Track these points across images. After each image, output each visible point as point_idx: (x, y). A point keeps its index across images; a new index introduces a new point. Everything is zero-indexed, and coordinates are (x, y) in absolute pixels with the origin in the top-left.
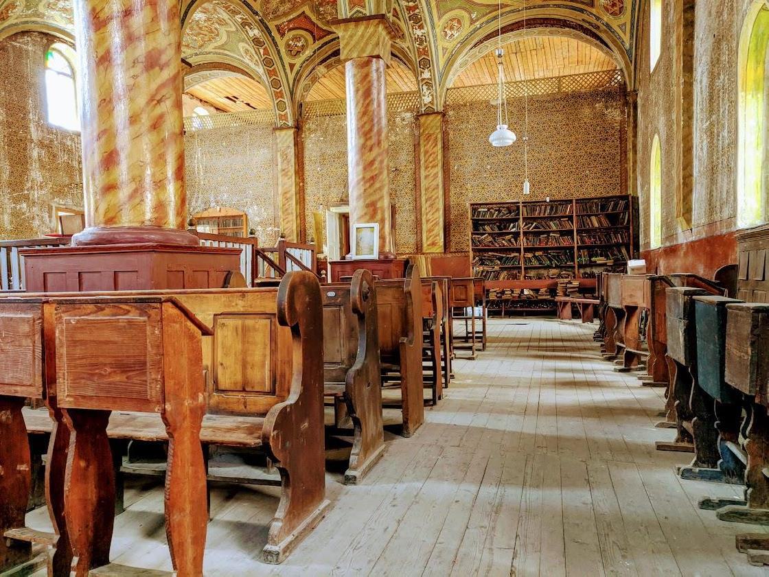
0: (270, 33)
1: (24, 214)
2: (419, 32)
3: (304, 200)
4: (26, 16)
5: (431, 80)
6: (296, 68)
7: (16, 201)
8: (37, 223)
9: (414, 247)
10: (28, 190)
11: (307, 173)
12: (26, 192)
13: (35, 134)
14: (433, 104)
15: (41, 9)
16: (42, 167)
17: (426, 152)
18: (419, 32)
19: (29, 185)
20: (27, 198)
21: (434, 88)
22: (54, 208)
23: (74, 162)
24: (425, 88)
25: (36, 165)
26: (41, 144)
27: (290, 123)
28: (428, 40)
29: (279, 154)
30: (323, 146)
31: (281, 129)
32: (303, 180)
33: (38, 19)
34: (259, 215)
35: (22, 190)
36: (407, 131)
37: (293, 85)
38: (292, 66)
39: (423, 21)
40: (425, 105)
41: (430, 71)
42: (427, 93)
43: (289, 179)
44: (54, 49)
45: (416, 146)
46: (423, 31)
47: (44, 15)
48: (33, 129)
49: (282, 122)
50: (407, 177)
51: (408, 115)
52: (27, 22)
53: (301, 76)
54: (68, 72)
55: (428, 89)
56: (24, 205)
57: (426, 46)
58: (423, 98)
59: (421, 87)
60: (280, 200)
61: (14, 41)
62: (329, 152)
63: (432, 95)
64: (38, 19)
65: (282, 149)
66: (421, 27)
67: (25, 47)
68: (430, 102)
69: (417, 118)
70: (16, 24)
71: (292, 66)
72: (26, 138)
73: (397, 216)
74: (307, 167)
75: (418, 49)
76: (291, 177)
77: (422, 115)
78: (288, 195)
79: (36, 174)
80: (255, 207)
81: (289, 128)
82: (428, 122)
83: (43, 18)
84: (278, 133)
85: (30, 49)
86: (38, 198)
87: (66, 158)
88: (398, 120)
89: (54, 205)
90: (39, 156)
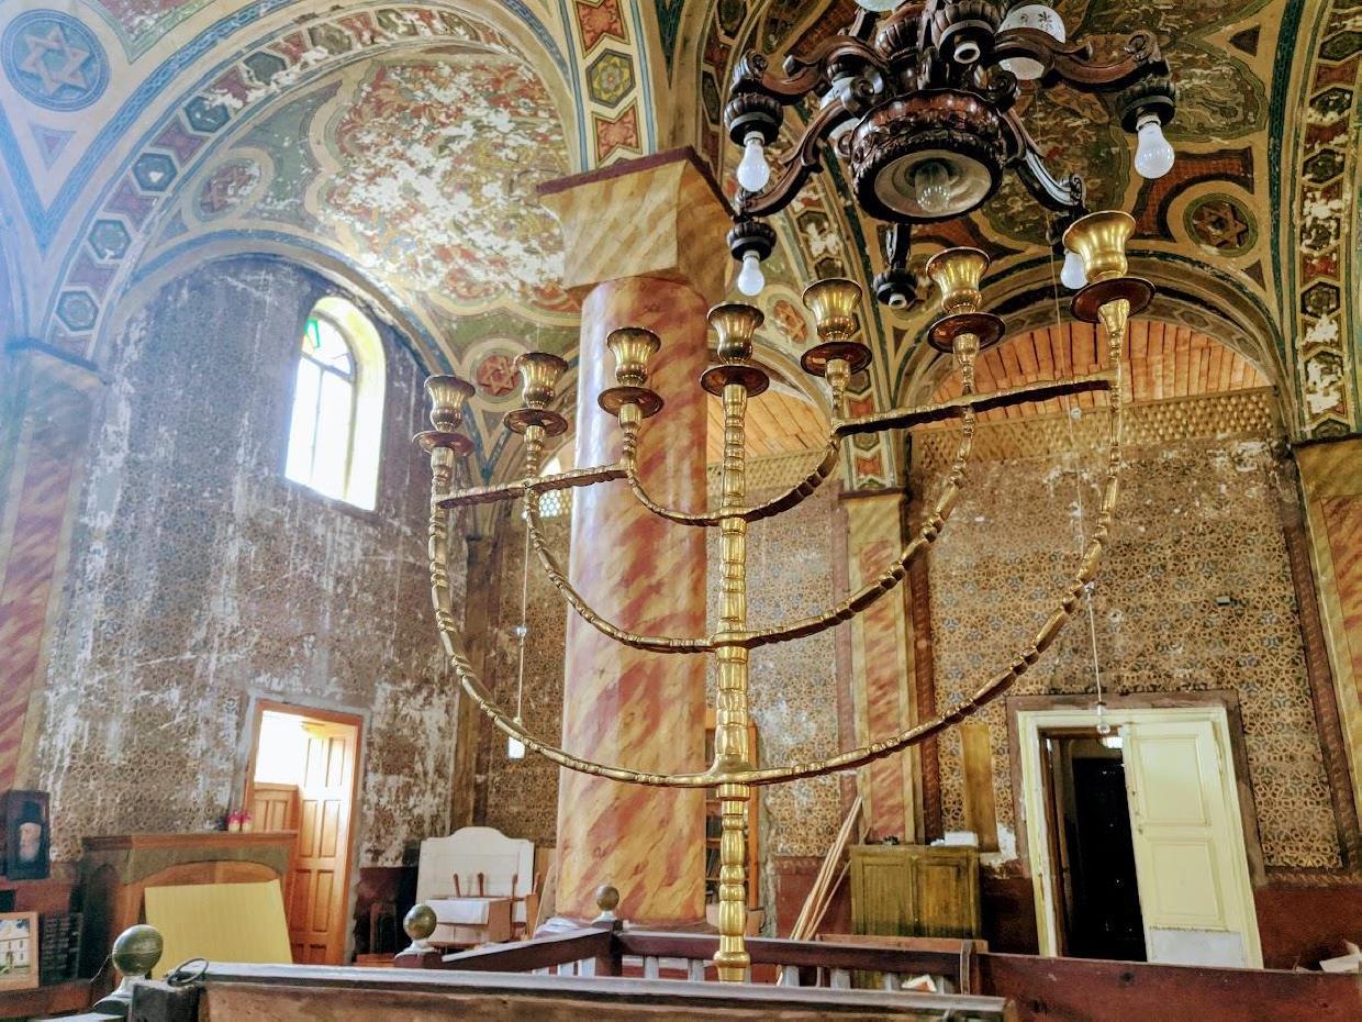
0: (861, 246)
1: (169, 717)
2: (1320, 209)
3: (933, 688)
4: (272, 216)
5: (1338, 345)
6: (907, 342)
7: (156, 680)
8: (201, 742)
9: (1332, 848)
10: (194, 650)
11: (938, 613)
12: (188, 655)
13: (242, 500)
14: (1343, 412)
15: (311, 203)
16: (245, 586)
17: (1337, 551)
18: (1320, 209)
19: (200, 635)
20: (186, 673)
21: (1347, 369)
22: (252, 703)
23: (324, 579)
24: (1315, 368)
25: (228, 581)
26: (254, 530)
27: (889, 479)
28: (1345, 229)
29: (854, 563)
30: (986, 538)
31: (863, 494)
32: (929, 633)
33: (300, 233)
34: (793, 727)
35: (178, 650)
36: (1255, 492)
37: (897, 388)
38: (899, 335)
39: (1345, 175)
40: (1314, 417)
41: (1338, 319)
42: (1320, 386)
43: (887, 628)
44: (321, 315)
45: (1294, 539)
46: (1335, 204)
47: (315, 221)
48: (238, 488)
49: (865, 479)
50: (1275, 618)
51: (1254, 447)
52: (270, 235)
53: (915, 363)
54: (345, 367)
55: (1327, 371)
56: (175, 694)
57: (1336, 250)
58: (1309, 397)
59: (1300, 366)
60: (860, 693)
61: (235, 275)
62: (1004, 554)
63: (1341, 390)
64: (300, 233)
65: (866, 549)
66: (1332, 193)
67: (257, 294)
68: (1333, 409)
69: (1287, 452)
70: (242, 234)
71: (899, 335)
72: (216, 510)
73: (1250, 741)
74: (938, 596)
75: (1306, 258)
76: (894, 623)
77: (1306, 444)
78: (886, 674)
79: (224, 607)
80: (784, 707)
81: (885, 492)
82: (1332, 463)
83: (310, 229)
84: (851, 506)
85: (268, 299)
86: (219, 671)
87: (307, 566)
88: (1220, 462)
89: (254, 694)
90: (242, 559)
